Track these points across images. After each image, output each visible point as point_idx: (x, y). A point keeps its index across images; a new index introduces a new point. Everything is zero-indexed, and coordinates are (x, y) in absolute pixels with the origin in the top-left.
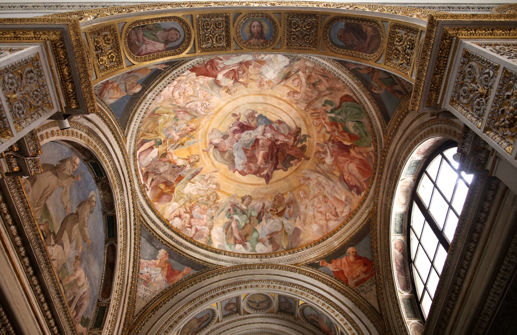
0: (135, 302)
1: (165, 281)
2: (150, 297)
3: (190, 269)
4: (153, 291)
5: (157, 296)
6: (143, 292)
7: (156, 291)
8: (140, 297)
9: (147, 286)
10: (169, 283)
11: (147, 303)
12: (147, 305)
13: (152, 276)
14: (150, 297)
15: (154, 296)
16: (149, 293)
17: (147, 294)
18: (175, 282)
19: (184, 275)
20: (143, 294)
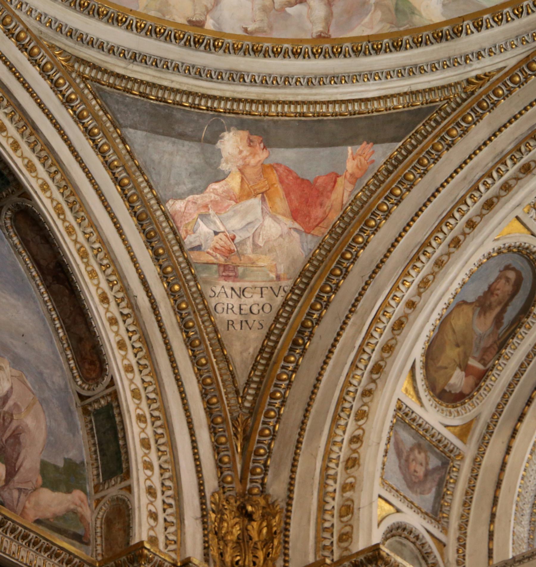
0: (222, 348)
1: (296, 235)
2: (267, 309)
3: (364, 148)
4: (268, 285)
5: (292, 291)
6: (234, 301)
7: (278, 278)
8: (230, 323)
9: (236, 278)
10: (316, 232)
11: (265, 331)
12: (268, 337)
13: (237, 239)
14: (267, 309)
15: (280, 300)
16: (257, 298)
17: (251, 301)
18: (334, 217)
19: (354, 179)
20: (236, 310)
